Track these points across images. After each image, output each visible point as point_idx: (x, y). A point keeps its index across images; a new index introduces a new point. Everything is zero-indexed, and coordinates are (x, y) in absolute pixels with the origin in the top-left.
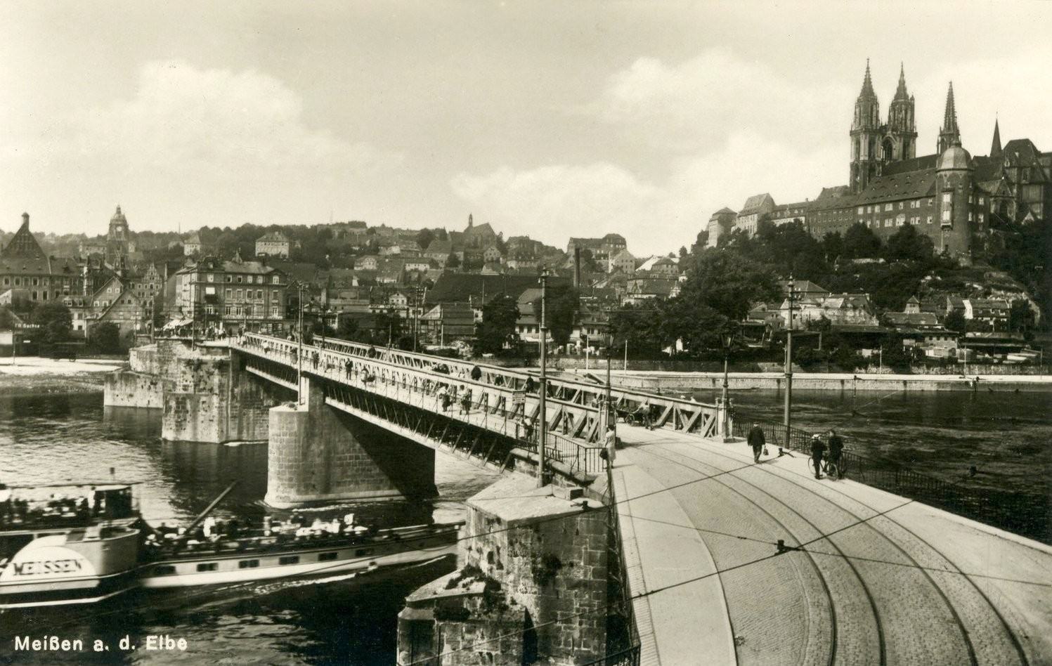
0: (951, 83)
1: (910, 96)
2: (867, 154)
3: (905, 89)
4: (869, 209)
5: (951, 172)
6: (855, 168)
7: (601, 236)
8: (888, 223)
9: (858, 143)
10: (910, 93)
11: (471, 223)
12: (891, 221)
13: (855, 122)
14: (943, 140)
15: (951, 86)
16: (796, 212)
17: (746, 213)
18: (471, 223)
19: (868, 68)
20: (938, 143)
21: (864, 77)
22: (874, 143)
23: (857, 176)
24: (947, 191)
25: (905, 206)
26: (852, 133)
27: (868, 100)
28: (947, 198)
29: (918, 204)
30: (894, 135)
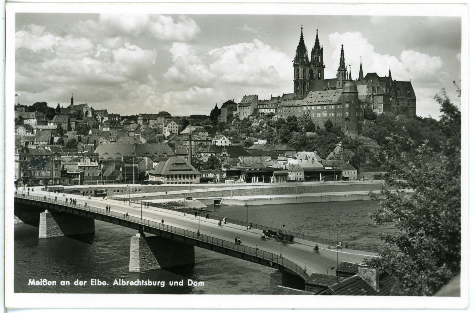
0: (342, 46)
1: (321, 47)
2: (302, 76)
6: (296, 83)
7: (158, 113)
8: (319, 115)
9: (298, 70)
10: (320, 45)
11: (72, 102)
12: (320, 114)
13: (296, 59)
14: (339, 73)
15: (342, 47)
16: (270, 106)
17: (242, 105)
18: (72, 102)
19: (302, 33)
20: (337, 74)
21: (300, 38)
22: (305, 71)
23: (297, 87)
24: (347, 103)
25: (326, 108)
27: (301, 48)
28: (347, 106)
29: (333, 106)
30: (314, 67)
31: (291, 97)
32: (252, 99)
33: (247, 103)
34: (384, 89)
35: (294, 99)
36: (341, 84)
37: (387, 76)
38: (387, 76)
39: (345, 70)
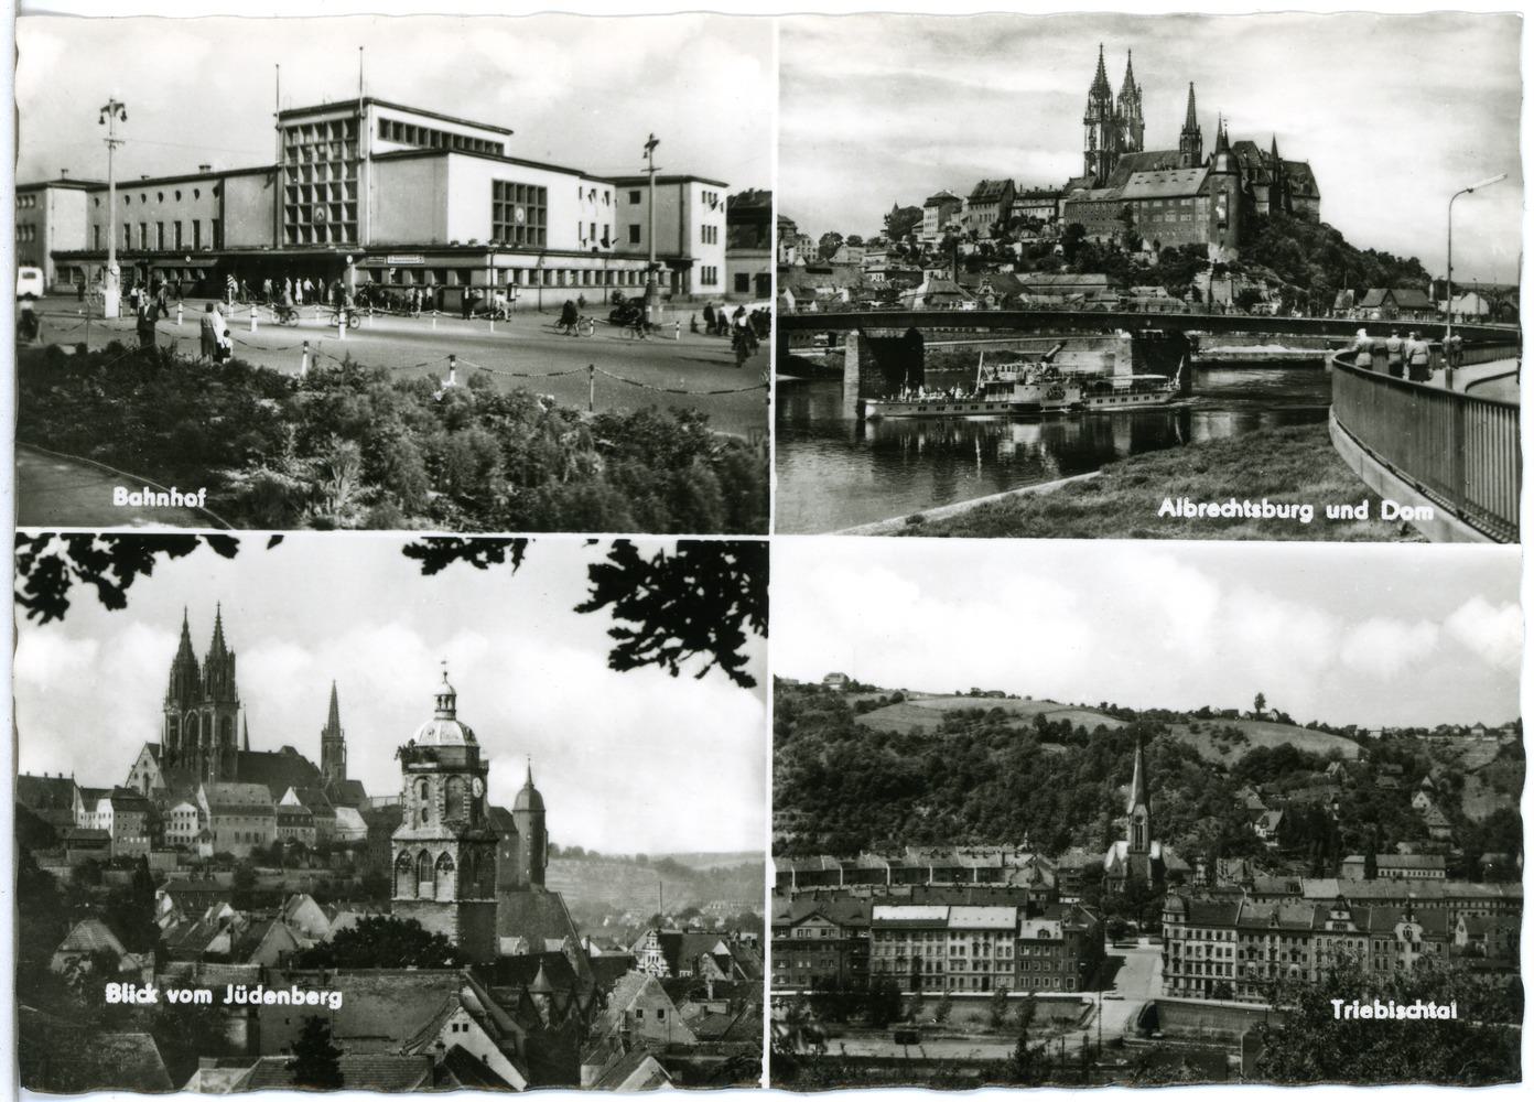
0: (1192, 84)
3: (1132, 80)
4: (1135, 203)
5: (1224, 176)
6: (1090, 156)
10: (1136, 82)
23: (1090, 165)
26: (1087, 122)
27: (1101, 88)
28: (1222, 199)
31: (1089, 183)
32: (1002, 187)
33: (991, 197)
34: (1270, 173)
35: (1098, 185)
36: (1189, 160)
37: (1269, 149)
38: (1269, 149)
39: (1198, 132)
